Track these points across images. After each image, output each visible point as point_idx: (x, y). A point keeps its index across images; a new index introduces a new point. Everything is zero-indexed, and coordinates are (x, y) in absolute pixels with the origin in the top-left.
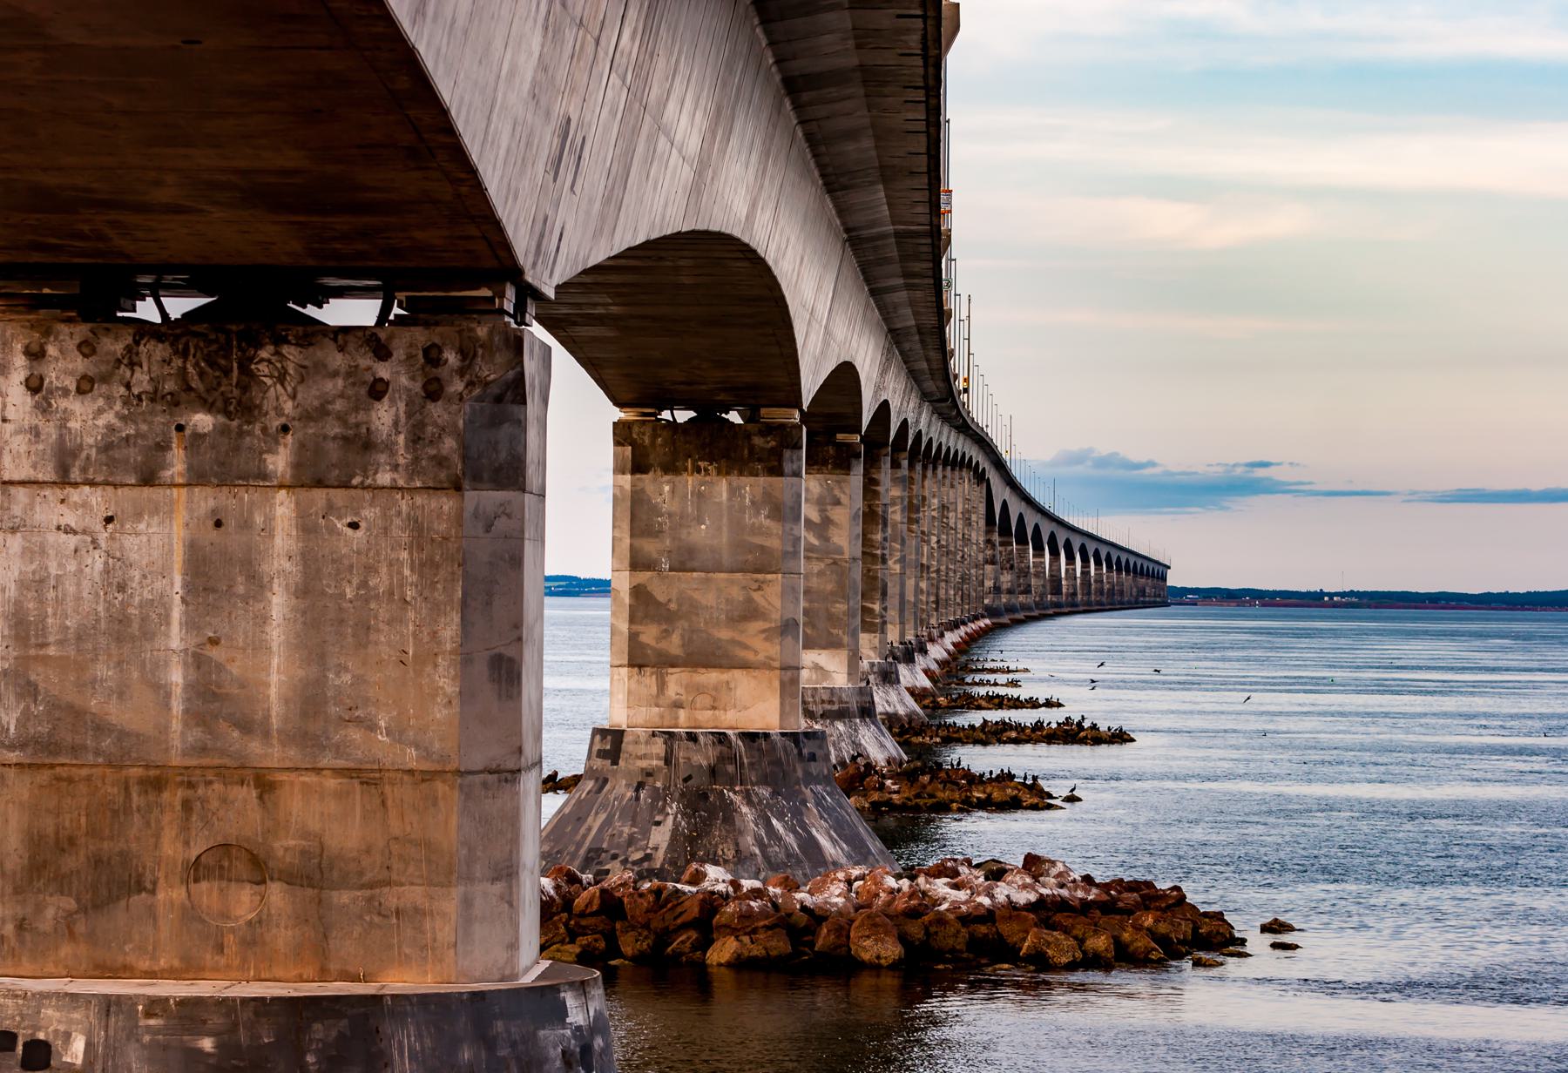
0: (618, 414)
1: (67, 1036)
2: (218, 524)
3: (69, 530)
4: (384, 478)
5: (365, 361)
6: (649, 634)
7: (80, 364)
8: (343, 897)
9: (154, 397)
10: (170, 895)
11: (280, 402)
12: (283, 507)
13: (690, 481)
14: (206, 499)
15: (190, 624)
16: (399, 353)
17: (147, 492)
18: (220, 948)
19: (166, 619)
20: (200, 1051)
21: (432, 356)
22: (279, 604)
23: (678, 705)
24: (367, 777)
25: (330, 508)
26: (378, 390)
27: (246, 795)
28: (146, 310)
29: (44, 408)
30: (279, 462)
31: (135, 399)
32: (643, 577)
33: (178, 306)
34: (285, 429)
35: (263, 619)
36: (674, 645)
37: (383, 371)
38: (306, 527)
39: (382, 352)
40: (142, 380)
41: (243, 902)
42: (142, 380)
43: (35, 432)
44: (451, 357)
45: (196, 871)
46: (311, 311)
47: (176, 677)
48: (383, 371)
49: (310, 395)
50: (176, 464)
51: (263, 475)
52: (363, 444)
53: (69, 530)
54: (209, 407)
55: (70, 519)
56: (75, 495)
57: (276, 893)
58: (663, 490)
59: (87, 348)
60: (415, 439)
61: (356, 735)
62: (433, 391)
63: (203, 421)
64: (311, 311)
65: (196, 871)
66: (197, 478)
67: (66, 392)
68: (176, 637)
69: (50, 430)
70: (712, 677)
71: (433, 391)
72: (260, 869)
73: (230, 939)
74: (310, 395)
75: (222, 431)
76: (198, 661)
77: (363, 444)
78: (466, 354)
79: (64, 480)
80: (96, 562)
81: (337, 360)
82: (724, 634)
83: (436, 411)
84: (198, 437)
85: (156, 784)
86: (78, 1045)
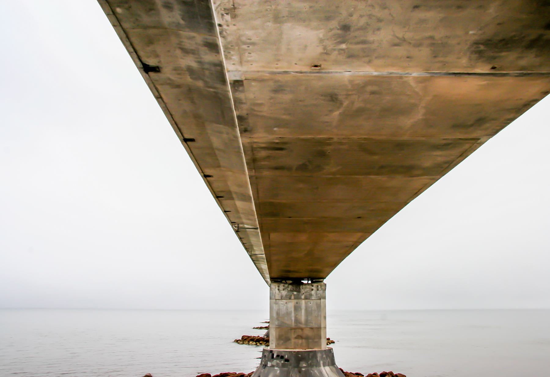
1: (285, 355)
2: (297, 303)
3: (282, 304)
4: (313, 298)
5: (311, 287)
8: (310, 341)
10: (293, 341)
11: (303, 291)
12: (303, 302)
14: (296, 301)
15: (295, 313)
16: (314, 286)
17: (290, 300)
18: (298, 346)
19: (292, 313)
20: (299, 357)
21: (317, 286)
22: (303, 311)
24: (312, 328)
25: (308, 302)
26: (312, 290)
27: (300, 330)
29: (280, 292)
30: (303, 297)
31: (288, 291)
34: (303, 294)
35: (302, 313)
37: (313, 288)
38: (306, 303)
40: (289, 289)
41: (300, 341)
43: (279, 294)
44: (319, 286)
45: (296, 338)
47: (293, 319)
48: (313, 288)
49: (306, 290)
50: (293, 297)
51: (301, 298)
53: (282, 304)
54: (296, 292)
55: (282, 303)
56: (282, 300)
57: (304, 340)
59: (284, 286)
60: (316, 294)
61: (311, 324)
62: (318, 290)
63: (295, 293)
66: (295, 299)
67: (282, 290)
68: (293, 314)
69: (280, 294)
71: (318, 290)
73: (299, 345)
74: (306, 290)
75: (297, 294)
76: (296, 317)
77: (311, 295)
78: (321, 286)
79: (282, 299)
80: (285, 307)
83: (318, 291)
84: (295, 295)
86: (287, 356)
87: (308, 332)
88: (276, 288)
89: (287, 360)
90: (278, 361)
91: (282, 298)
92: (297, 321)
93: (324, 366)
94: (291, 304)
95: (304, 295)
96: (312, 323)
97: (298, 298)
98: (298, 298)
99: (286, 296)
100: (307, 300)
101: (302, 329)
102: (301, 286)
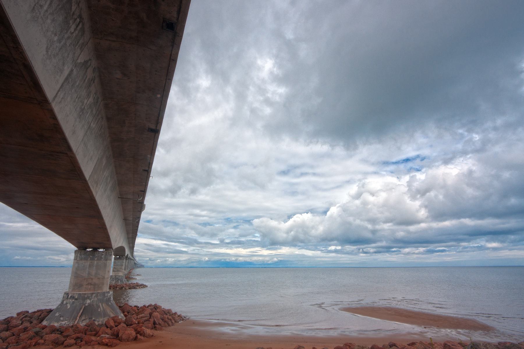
1: (76, 296)
5: (102, 253)
6: (115, 270)
7: (83, 253)
8: (96, 286)
9: (88, 255)
13: (118, 261)
14: (91, 261)
18: (87, 290)
20: (85, 297)
21: (106, 253)
23: (116, 274)
24: (99, 279)
26: (103, 255)
28: (88, 250)
30: (96, 259)
32: (115, 266)
33: (90, 250)
36: (116, 270)
37: (103, 254)
41: (90, 287)
43: (80, 257)
44: (108, 253)
46: (99, 250)
47: (87, 272)
48: (103, 254)
51: (95, 260)
52: (101, 258)
54: (91, 255)
58: (117, 261)
61: (99, 276)
63: (91, 256)
64: (99, 250)
65: (87, 285)
66: (90, 260)
72: (91, 284)
73: (88, 289)
77: (101, 258)
81: (100, 253)
82: (120, 270)
84: (91, 257)
85: (84, 279)
87: (95, 281)
88: (78, 253)
89: (76, 299)
91: (81, 260)
92: (89, 274)
94: (88, 263)
96: (99, 275)
98: (92, 259)
100: (98, 261)
101: (92, 279)
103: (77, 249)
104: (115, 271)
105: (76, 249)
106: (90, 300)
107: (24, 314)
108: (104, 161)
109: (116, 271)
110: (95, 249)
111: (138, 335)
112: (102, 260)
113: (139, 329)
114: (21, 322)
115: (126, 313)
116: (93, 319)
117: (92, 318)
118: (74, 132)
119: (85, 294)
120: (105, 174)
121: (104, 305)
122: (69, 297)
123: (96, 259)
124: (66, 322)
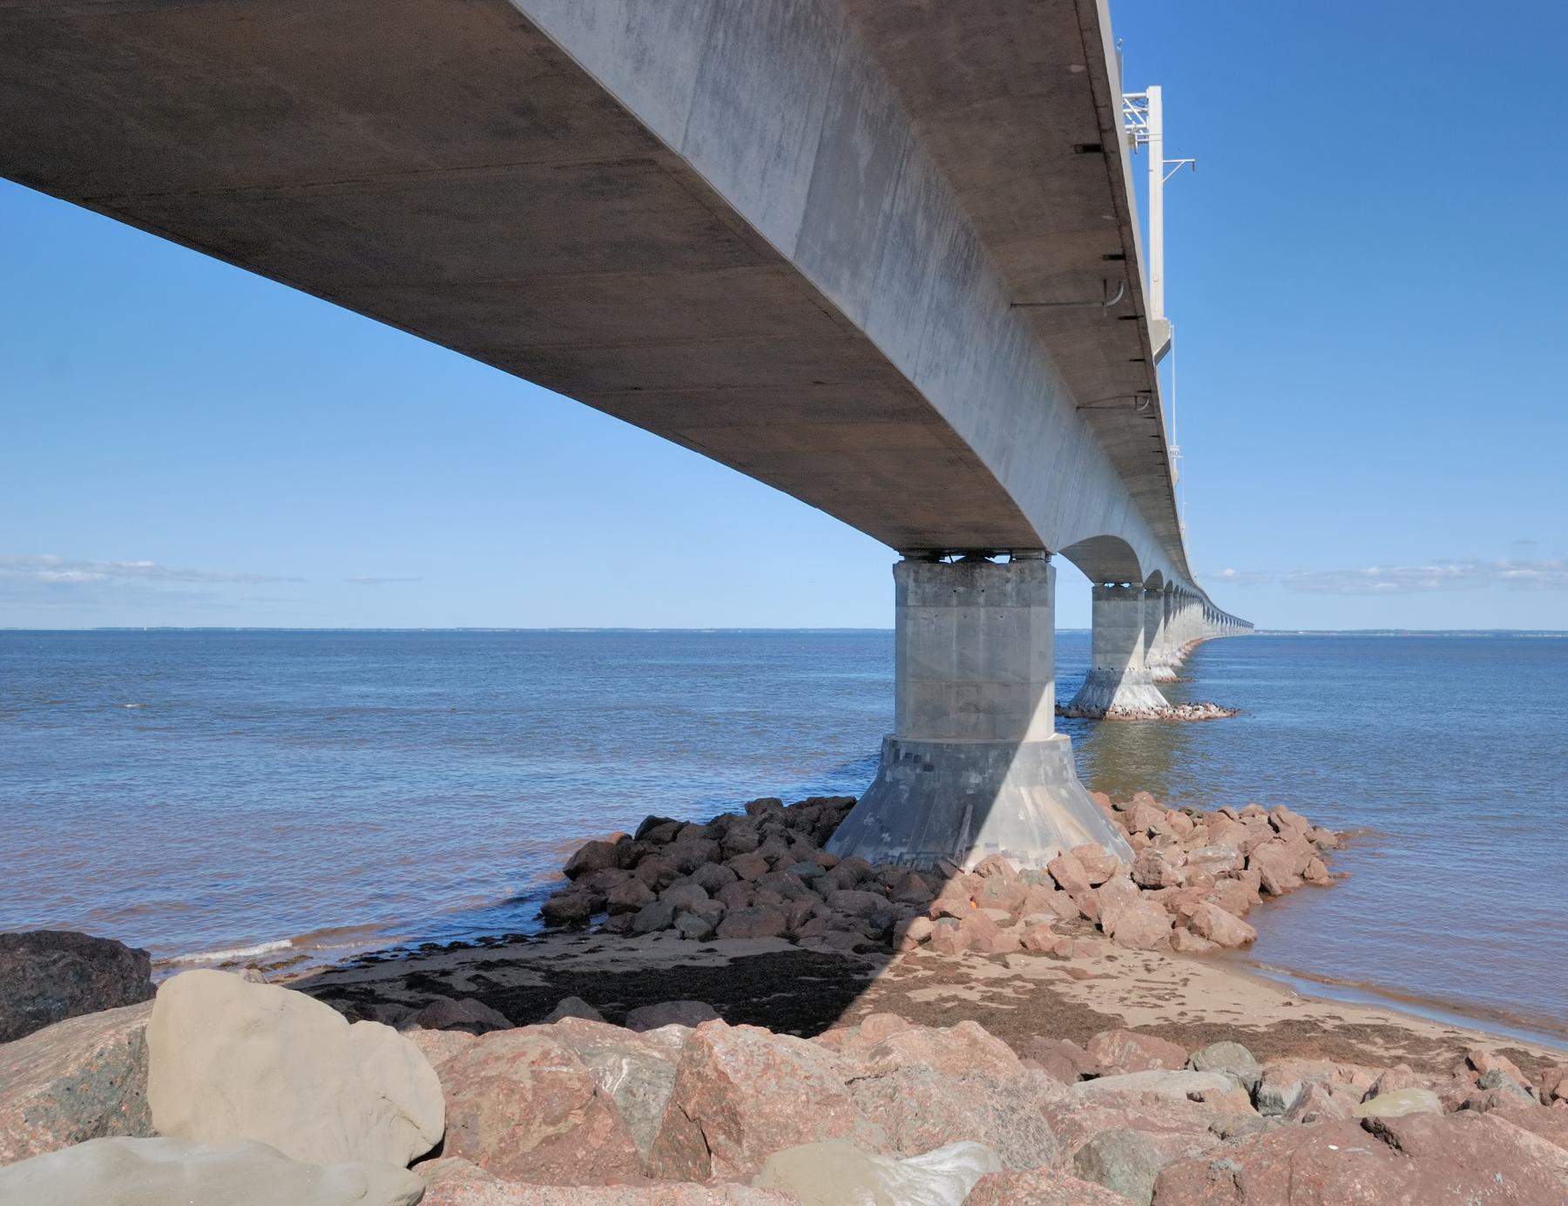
0: (1093, 585)
5: (1004, 573)
7: (928, 575)
9: (948, 583)
11: (982, 584)
12: (983, 614)
14: (962, 610)
20: (960, 758)
21: (1022, 571)
22: (981, 637)
24: (1006, 685)
26: (1007, 580)
28: (947, 560)
30: (982, 600)
33: (955, 558)
37: (1009, 575)
39: (1008, 570)
41: (973, 717)
42: (944, 578)
43: (917, 593)
44: (1027, 571)
45: (961, 710)
46: (991, 559)
47: (955, 657)
48: (1009, 575)
50: (954, 600)
51: (978, 604)
54: (962, 585)
57: (981, 715)
58: (1105, 605)
60: (1018, 592)
63: (961, 589)
64: (991, 559)
65: (961, 710)
66: (960, 604)
68: (954, 647)
69: (920, 591)
70: (1118, 656)
78: (1031, 570)
79: (924, 605)
80: (933, 627)
81: (997, 572)
83: (1024, 586)
84: (960, 594)
85: (950, 687)
88: (908, 576)
90: (908, 770)
91: (924, 602)
93: (1032, 781)
94: (952, 618)
95: (984, 594)
96: (1006, 670)
97: (967, 602)
99: (937, 596)
101: (978, 687)
102: (978, 570)
103: (902, 558)
104: (1107, 652)
105: (897, 557)
106: (981, 772)
107: (765, 811)
108: (862, 144)
109: (1109, 652)
110: (977, 556)
111: (1182, 931)
112: (1009, 604)
113: (1186, 909)
114: (757, 837)
115: (1142, 837)
116: (1002, 848)
117: (996, 845)
118: (641, 60)
119: (958, 748)
120: (886, 206)
121: (1037, 796)
122: (901, 758)
123: (982, 600)
124: (904, 850)
